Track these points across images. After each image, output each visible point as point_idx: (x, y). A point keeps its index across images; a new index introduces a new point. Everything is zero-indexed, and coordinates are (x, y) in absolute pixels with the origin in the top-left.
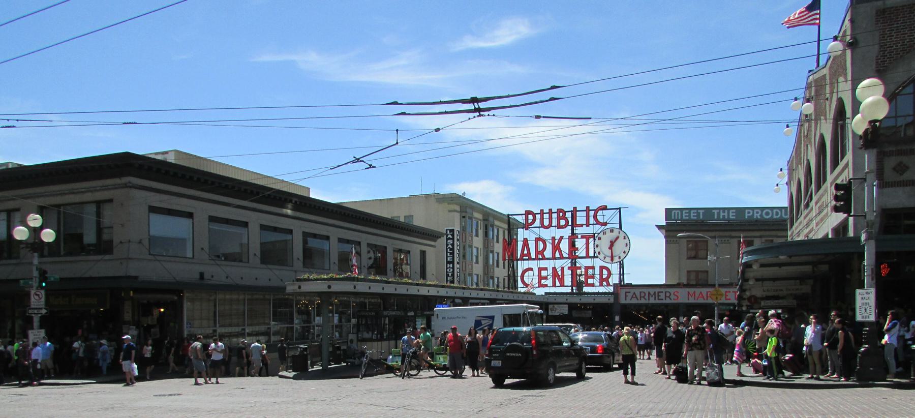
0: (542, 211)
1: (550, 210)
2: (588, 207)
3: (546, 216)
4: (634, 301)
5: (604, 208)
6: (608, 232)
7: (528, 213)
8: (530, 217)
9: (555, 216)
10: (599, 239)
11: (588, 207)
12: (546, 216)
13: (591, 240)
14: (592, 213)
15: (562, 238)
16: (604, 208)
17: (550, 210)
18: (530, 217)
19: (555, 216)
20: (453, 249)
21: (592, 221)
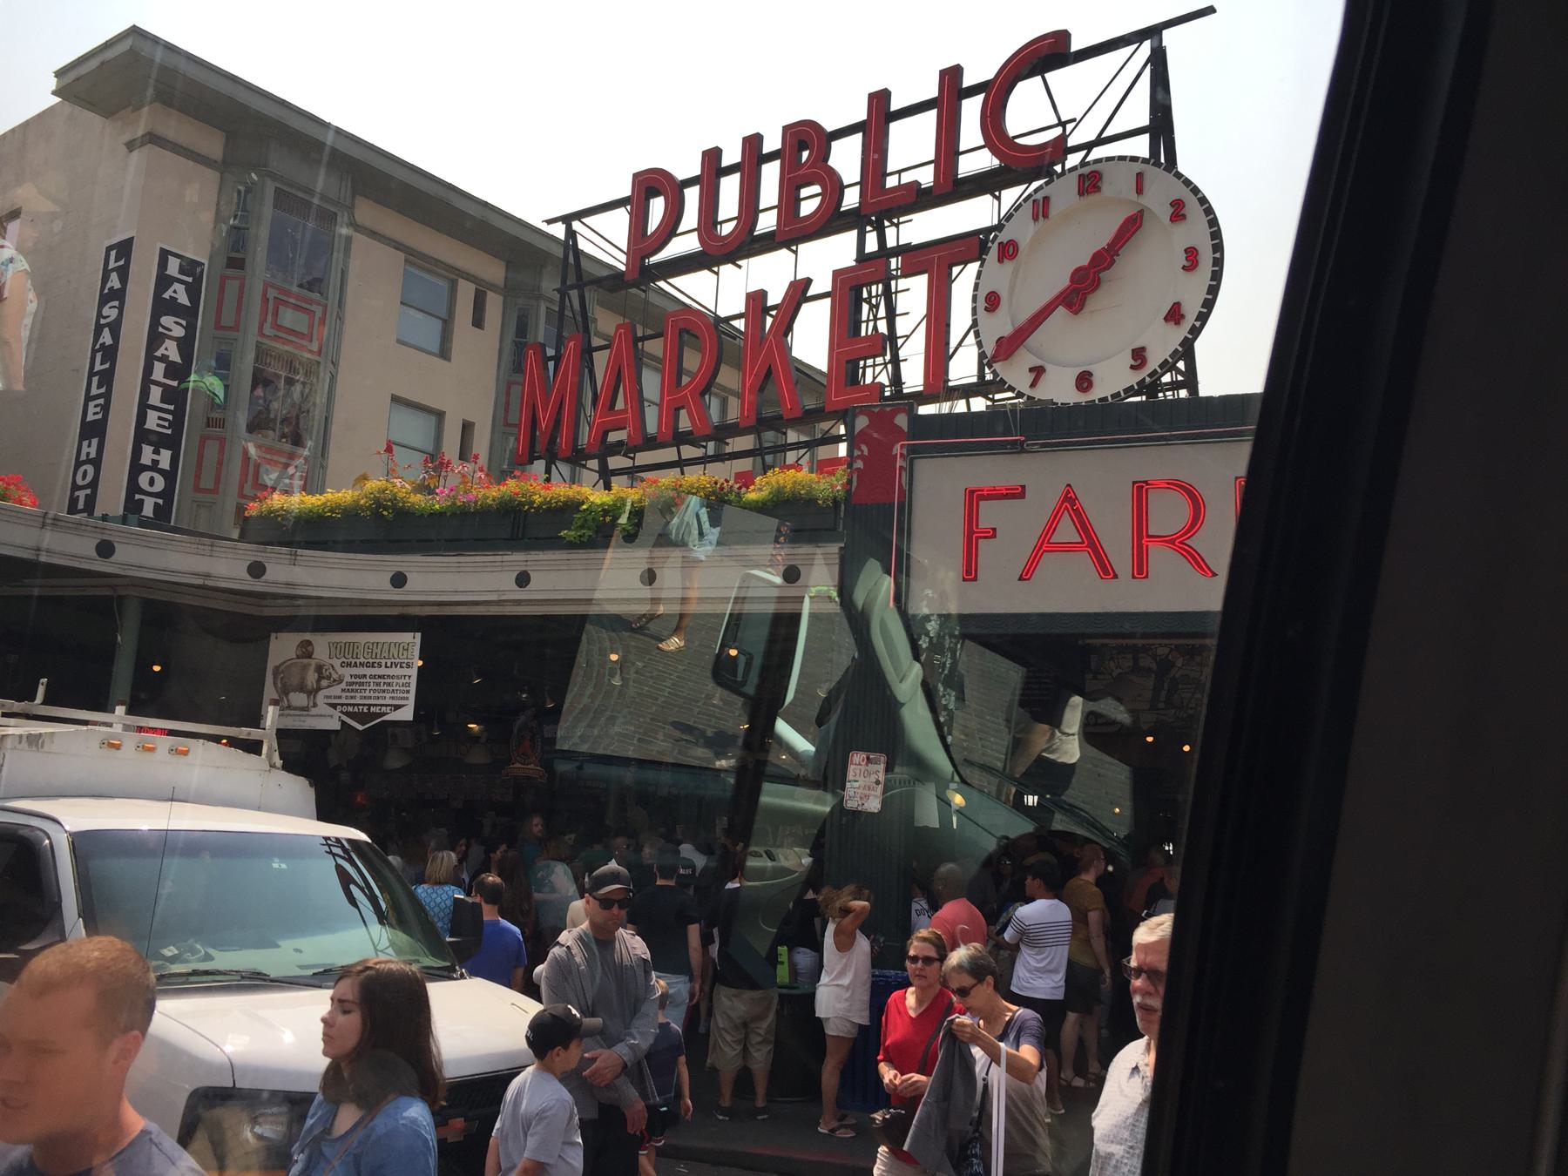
0: (712, 157)
1: (752, 143)
2: (951, 77)
3: (730, 188)
4: (1069, 590)
5: (1048, 54)
6: (1064, 193)
7: (651, 183)
8: (657, 207)
9: (771, 174)
10: (1008, 251)
11: (951, 77)
12: (730, 188)
13: (964, 281)
14: (971, 109)
15: (799, 292)
16: (1048, 54)
17: (752, 143)
18: (657, 207)
19: (771, 174)
20: (110, 353)
21: (976, 161)
